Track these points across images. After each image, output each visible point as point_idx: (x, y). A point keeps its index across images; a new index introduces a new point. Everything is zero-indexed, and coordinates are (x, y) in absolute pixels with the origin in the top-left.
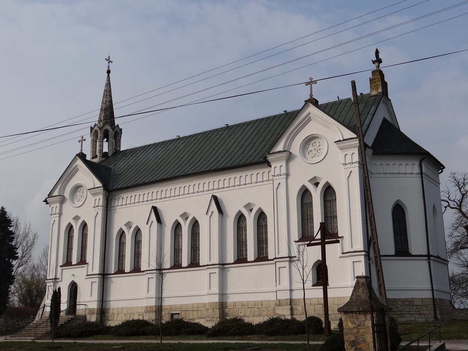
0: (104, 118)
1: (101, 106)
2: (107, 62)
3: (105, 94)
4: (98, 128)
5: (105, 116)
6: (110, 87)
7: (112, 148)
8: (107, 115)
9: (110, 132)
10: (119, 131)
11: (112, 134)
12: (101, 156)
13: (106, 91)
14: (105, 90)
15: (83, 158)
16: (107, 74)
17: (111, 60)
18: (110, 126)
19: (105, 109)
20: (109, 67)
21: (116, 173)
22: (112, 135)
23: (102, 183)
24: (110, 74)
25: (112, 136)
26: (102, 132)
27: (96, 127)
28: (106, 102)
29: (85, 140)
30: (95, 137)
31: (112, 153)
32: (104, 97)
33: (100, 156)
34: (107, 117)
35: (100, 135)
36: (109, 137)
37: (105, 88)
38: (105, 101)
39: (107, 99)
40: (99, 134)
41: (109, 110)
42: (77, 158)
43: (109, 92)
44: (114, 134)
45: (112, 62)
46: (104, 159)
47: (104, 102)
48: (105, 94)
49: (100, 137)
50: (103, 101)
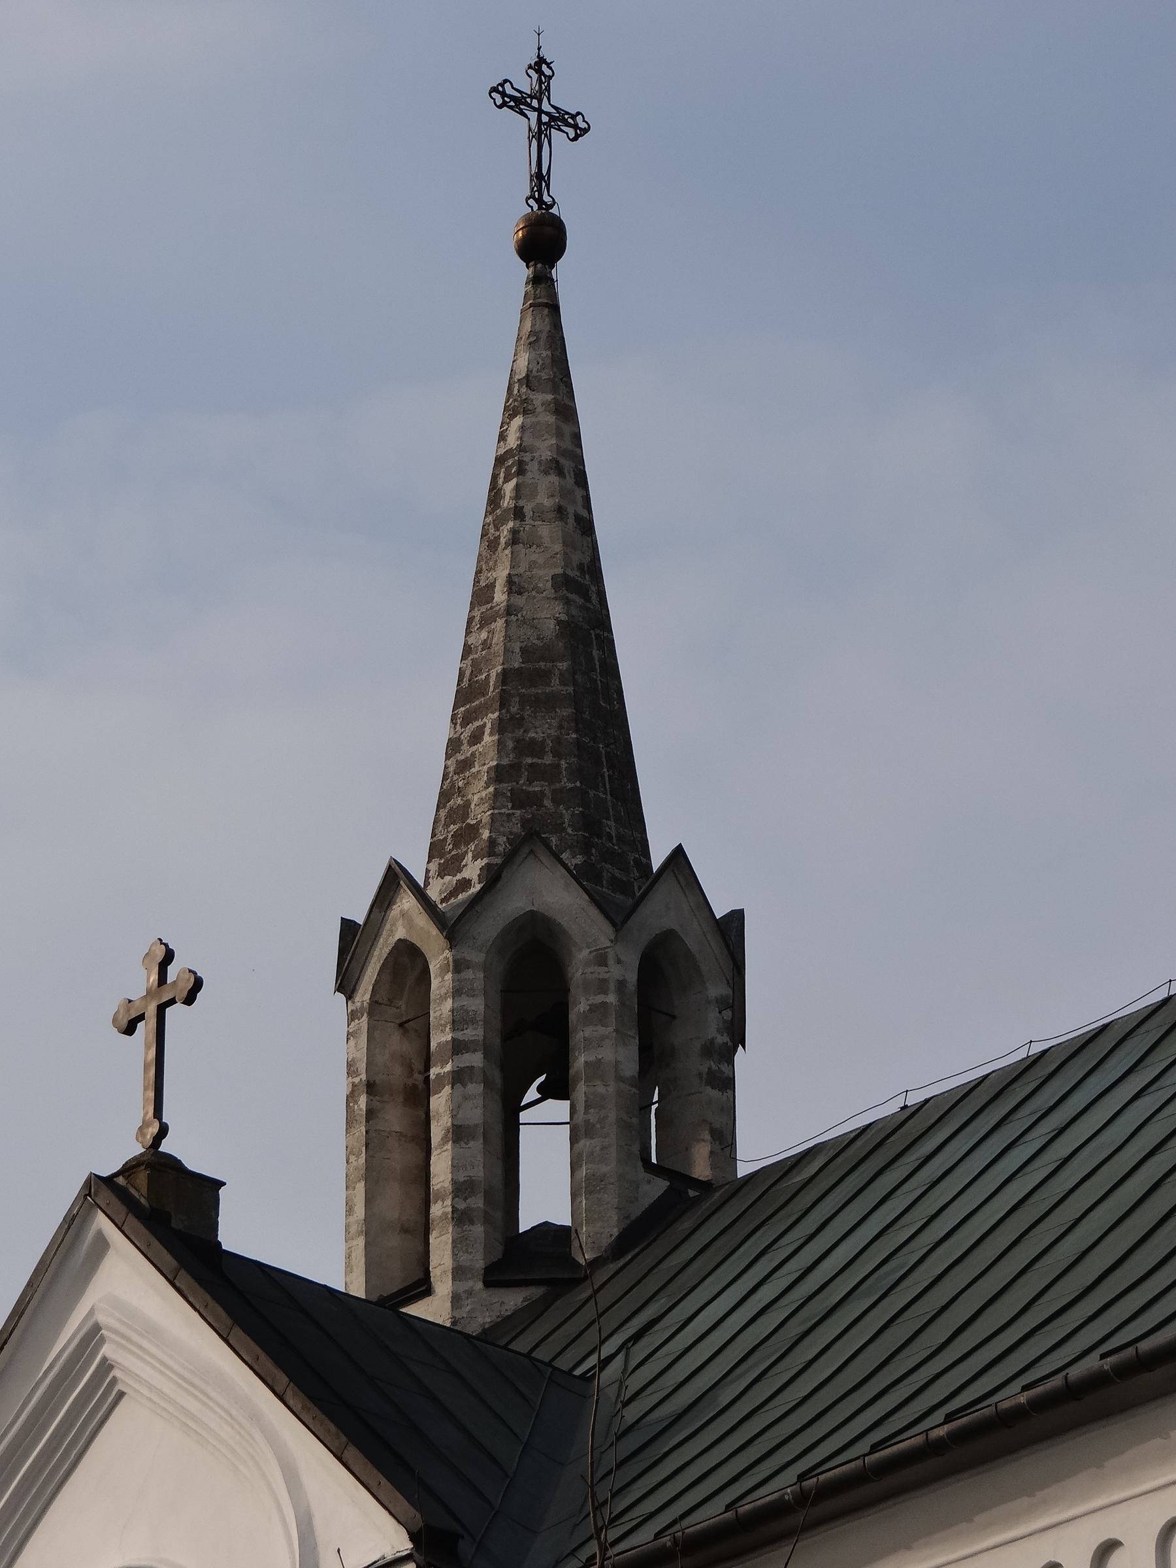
0: (506, 787)
1: (467, 650)
2: (517, 126)
3: (507, 502)
4: (422, 920)
5: (515, 767)
6: (566, 412)
7: (613, 1153)
8: (534, 748)
9: (584, 954)
10: (696, 939)
11: (614, 972)
12: (480, 1264)
13: (521, 463)
14: (509, 453)
15: (177, 1223)
16: (521, 272)
17: (562, 96)
18: (584, 877)
19: (505, 676)
20: (540, 179)
21: (631, 1414)
22: (602, 986)
23: (403, 1505)
24: (563, 271)
25: (611, 998)
26: (478, 957)
27: (406, 902)
28: (520, 601)
29: (198, 984)
30: (396, 1043)
31: (614, 1216)
32: (490, 544)
33: (458, 1272)
34: (537, 773)
35: (457, 993)
36: (573, 1017)
37: (502, 437)
38: (513, 585)
39: (535, 555)
40: (440, 983)
41: (555, 684)
42: (90, 1235)
43: (560, 472)
44: (632, 978)
45: (580, 132)
46: (513, 1300)
47: (500, 596)
48: (507, 502)
49: (458, 1020)
50: (481, 594)
